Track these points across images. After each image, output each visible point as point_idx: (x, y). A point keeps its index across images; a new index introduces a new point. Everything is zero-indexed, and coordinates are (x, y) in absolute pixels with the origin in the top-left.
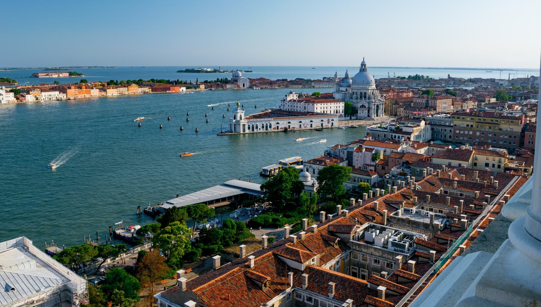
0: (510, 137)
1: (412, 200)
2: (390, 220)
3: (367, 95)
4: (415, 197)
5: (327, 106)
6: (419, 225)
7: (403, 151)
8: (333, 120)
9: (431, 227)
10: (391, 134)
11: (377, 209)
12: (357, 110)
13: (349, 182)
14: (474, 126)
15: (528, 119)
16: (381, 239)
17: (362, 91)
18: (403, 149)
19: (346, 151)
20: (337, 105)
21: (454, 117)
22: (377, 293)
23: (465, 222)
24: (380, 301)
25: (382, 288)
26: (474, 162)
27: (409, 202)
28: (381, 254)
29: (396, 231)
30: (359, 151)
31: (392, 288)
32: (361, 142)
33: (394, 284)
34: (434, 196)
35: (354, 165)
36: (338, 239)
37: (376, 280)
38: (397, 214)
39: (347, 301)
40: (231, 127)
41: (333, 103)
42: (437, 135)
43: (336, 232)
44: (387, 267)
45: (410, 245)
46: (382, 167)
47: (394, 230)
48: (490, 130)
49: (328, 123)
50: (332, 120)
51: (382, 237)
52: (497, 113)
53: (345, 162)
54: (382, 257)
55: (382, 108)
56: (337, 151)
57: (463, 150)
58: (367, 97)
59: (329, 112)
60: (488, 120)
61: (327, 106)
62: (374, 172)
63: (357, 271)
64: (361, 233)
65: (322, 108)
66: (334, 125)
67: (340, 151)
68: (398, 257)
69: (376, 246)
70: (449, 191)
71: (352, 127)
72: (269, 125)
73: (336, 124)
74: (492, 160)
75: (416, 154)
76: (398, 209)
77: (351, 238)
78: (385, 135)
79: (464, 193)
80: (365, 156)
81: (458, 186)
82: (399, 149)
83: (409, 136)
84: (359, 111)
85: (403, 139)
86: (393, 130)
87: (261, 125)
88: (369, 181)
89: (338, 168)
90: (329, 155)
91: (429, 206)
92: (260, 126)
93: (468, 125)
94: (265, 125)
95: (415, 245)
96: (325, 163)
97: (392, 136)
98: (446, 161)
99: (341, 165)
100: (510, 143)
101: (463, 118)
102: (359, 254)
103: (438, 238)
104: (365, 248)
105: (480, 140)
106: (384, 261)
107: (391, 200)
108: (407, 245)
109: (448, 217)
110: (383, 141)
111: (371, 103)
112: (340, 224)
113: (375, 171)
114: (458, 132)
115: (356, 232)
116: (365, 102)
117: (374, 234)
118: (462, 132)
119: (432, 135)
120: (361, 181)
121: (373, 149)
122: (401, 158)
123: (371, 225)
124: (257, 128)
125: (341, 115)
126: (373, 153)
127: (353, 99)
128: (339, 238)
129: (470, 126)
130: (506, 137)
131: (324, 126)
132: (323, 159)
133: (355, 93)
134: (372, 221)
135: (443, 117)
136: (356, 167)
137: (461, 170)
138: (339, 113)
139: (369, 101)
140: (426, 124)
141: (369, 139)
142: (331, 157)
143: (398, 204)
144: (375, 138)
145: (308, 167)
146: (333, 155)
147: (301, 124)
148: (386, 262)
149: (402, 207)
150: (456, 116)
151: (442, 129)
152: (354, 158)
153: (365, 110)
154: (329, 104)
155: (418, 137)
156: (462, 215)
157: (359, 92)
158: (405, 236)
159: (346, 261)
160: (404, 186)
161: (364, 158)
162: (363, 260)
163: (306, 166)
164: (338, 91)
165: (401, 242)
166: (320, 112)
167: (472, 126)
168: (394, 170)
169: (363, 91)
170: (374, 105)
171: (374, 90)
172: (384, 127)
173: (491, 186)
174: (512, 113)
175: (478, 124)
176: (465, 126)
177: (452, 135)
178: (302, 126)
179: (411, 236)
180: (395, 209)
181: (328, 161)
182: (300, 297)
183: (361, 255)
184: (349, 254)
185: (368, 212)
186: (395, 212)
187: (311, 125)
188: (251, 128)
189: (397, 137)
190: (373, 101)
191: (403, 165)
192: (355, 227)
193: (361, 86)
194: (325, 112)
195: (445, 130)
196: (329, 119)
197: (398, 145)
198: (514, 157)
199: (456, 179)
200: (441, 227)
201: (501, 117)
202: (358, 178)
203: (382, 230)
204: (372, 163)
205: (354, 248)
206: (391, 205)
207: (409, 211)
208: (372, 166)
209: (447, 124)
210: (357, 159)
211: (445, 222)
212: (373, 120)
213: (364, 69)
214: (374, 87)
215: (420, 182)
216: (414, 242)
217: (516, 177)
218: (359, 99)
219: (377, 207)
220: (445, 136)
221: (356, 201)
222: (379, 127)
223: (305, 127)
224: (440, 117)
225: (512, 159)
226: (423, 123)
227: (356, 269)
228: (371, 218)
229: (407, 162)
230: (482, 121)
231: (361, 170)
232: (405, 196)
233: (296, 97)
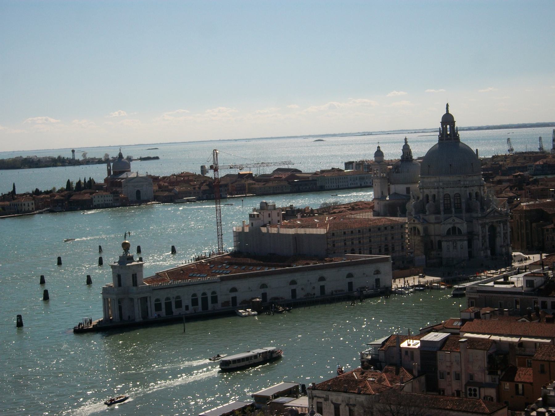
12: (440, 243)
17: (448, 191)
32: (455, 324)
35: (442, 384)
55: (505, 234)
58: (464, 206)
62: (495, 401)
65: (349, 243)
72: (209, 296)
84: (444, 244)
86: (538, 288)
87: (190, 297)
92: (187, 301)
124: (179, 304)
127: (427, 213)
133: (430, 198)
136: (448, 391)
145: (320, 400)
147: (293, 287)
153: (460, 240)
163: (315, 399)
170: (483, 226)
178: (297, 291)
187: (322, 288)
188: (163, 306)
190: (480, 215)
218: (442, 213)
223: (308, 294)
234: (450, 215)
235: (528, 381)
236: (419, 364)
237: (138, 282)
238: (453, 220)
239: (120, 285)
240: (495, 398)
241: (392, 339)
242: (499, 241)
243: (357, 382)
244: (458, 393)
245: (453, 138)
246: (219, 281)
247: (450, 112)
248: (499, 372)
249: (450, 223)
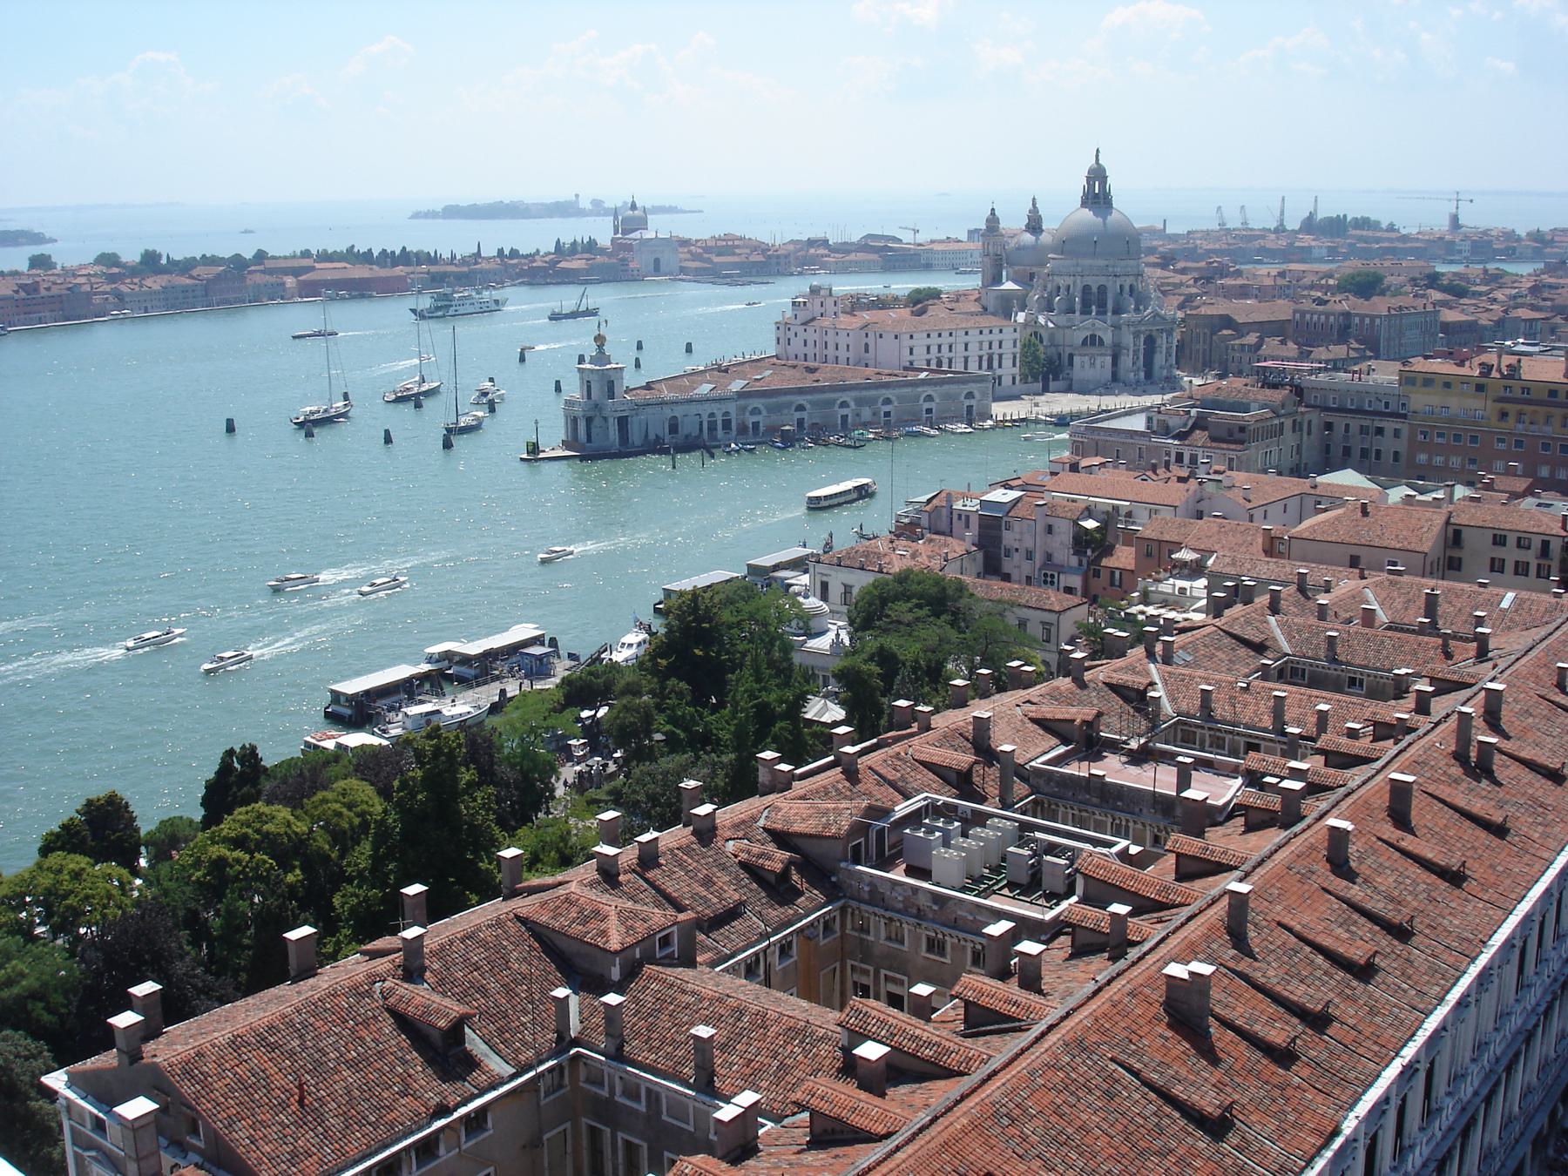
5: (952, 340)
9: (1179, 811)
12: (1071, 357)
17: (1089, 281)
20: (991, 337)
26: (1450, 553)
35: (1007, 565)
40: (575, 429)
47: (1016, 821)
54: (954, 928)
58: (1110, 306)
59: (959, 366)
61: (952, 340)
62: (1079, 593)
65: (934, 349)
70: (1307, 668)
79: (1365, 678)
84: (1077, 360)
88: (1053, 630)
91: (1210, 729)
94: (705, 419)
102: (876, 915)
106: (962, 942)
111: (1124, 328)
116: (1099, 323)
136: (1015, 575)
138: (1000, 366)
139: (1116, 318)
145: (825, 579)
148: (970, 945)
153: (1101, 355)
157: (1079, 286)
162: (889, 938)
170: (1136, 335)
175: (1501, 405)
182: (601, 1084)
184: (837, 914)
189: (1186, 459)
193: (1087, 262)
194: (945, 368)
218: (1078, 313)
227: (866, 972)
233: (835, 309)
234: (1088, 317)
235: (1129, 568)
236: (977, 533)
237: (616, 395)
238: (1093, 325)
239: (589, 396)
240: (1079, 588)
241: (943, 495)
242: (1159, 359)
243: (879, 556)
245: (1102, 201)
246: (735, 397)
248: (1089, 552)
249: (1087, 329)
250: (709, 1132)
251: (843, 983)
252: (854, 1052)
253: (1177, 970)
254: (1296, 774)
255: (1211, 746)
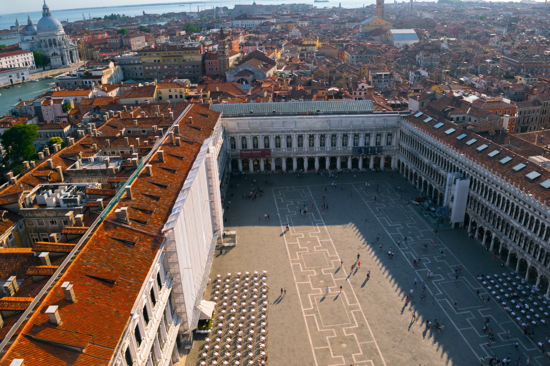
0: (194, 66)
1: (92, 148)
2: (68, 174)
3: (57, 42)
4: (94, 144)
5: (13, 59)
6: (97, 173)
7: (95, 96)
8: (22, 74)
9: (108, 172)
10: (81, 80)
11: (52, 167)
12: (49, 59)
13: (41, 139)
14: (161, 61)
15: (206, 48)
16: (52, 199)
17: (50, 38)
18: (94, 94)
19: (33, 107)
21: (141, 55)
22: (42, 261)
23: (135, 160)
24: (42, 268)
25: (44, 255)
26: (160, 95)
27: (90, 150)
28: (55, 214)
29: (68, 186)
30: (47, 104)
31: (58, 250)
33: (59, 246)
34: (114, 139)
35: (45, 119)
36: (5, 211)
37: (41, 247)
38: (74, 167)
39: (9, 280)
41: (20, 55)
42: (128, 74)
43: (2, 205)
44: (65, 224)
45: (83, 197)
46: (75, 116)
47: (66, 185)
48: (176, 63)
49: (19, 77)
50: (22, 74)
51: (53, 197)
52: (179, 46)
53: (35, 118)
55: (76, 54)
56: (23, 108)
57: (147, 87)
58: (57, 44)
59: (17, 66)
60: (172, 53)
61: (13, 59)
63: (37, 237)
64: (33, 198)
65: (8, 62)
66: (25, 79)
67: (27, 108)
68: (67, 214)
69: (49, 207)
70: (131, 130)
71: (46, 78)
73: (28, 77)
74: (176, 91)
75: (105, 97)
76: (75, 161)
77: (21, 206)
78: (75, 82)
80: (54, 109)
81: (139, 124)
82: (90, 95)
83: (99, 80)
84: (51, 60)
85: (94, 84)
88: (62, 133)
89: (21, 128)
90: (15, 115)
93: (155, 61)
95: (88, 196)
96: (11, 125)
97: (83, 82)
98: (132, 100)
99: (29, 123)
100: (194, 72)
101: (150, 54)
103: (111, 183)
104: (38, 213)
105: (168, 73)
107: (68, 153)
108: (78, 198)
109: (123, 159)
110: (73, 89)
111: (63, 50)
112: (8, 194)
113: (69, 123)
114: (147, 68)
115: (25, 199)
116: (55, 49)
117: (46, 196)
118: (151, 68)
119: (124, 75)
120: (51, 136)
121: (62, 100)
122: (91, 104)
123: (42, 186)
125: (32, 67)
126: (62, 103)
128: (5, 209)
129: (157, 61)
130: (190, 67)
131: (14, 82)
132: (8, 121)
133: (43, 41)
134: (47, 181)
135: (131, 56)
136: (48, 122)
137: (145, 106)
140: (115, 65)
141: (58, 89)
142: (18, 116)
143: (75, 156)
144: (66, 87)
146: (19, 114)
148: (62, 220)
149: (80, 158)
150: (143, 53)
151: (132, 68)
152: (43, 112)
154: (15, 57)
155: (110, 79)
156: (134, 154)
158: (79, 188)
159: (21, 231)
160: (84, 135)
161: (54, 112)
162: (39, 224)
164: (23, 41)
165: (72, 196)
166: (6, 67)
167: (159, 61)
168: (86, 116)
169: (52, 38)
170: (67, 51)
171: (63, 35)
172: (73, 75)
173: (168, 118)
174: (192, 45)
176: (153, 61)
177: (142, 71)
179: (85, 187)
180: (73, 162)
181: (14, 121)
183: (36, 221)
184: (23, 222)
185: (41, 173)
186: (73, 165)
189: (88, 82)
191: (95, 111)
192: (23, 194)
194: (13, 67)
195: (136, 68)
196: (18, 74)
197: (87, 91)
198: (196, 85)
199: (139, 117)
200: (116, 170)
201: (183, 48)
202: (50, 133)
203: (54, 188)
204: (64, 114)
205: (26, 215)
206: (68, 159)
207: (87, 160)
208: (65, 117)
209: (136, 62)
210: (47, 113)
211: (122, 164)
212: (69, 67)
213: (47, 14)
214: (62, 31)
215: (100, 128)
216: (86, 194)
217: (190, 105)
219: (52, 165)
220: (136, 74)
221: (30, 164)
222: (68, 75)
224: (128, 56)
225: (195, 87)
226: (111, 64)
228: (45, 178)
229: (98, 106)
230: (168, 55)
231: (54, 124)
232: (84, 146)
242: (74, 57)
244: (52, 121)
247: (46, 4)
250: (3, 290)
251: (30, 240)
252: (39, 256)
253: (118, 211)
254: (135, 156)
255: (112, 154)
